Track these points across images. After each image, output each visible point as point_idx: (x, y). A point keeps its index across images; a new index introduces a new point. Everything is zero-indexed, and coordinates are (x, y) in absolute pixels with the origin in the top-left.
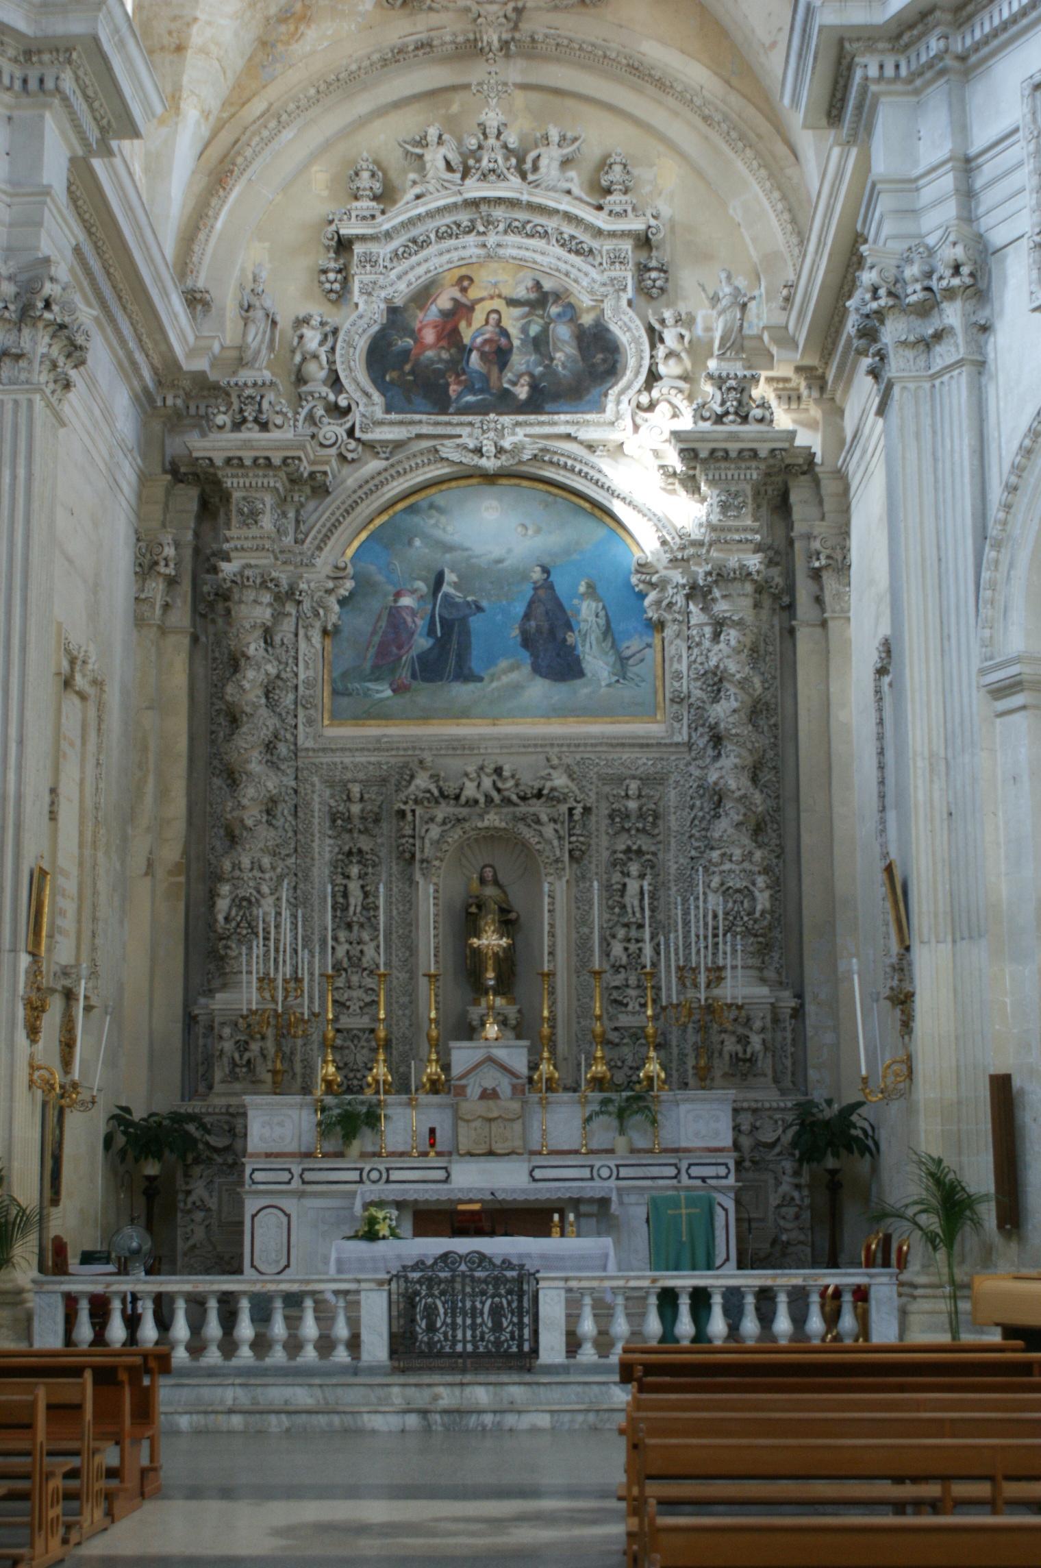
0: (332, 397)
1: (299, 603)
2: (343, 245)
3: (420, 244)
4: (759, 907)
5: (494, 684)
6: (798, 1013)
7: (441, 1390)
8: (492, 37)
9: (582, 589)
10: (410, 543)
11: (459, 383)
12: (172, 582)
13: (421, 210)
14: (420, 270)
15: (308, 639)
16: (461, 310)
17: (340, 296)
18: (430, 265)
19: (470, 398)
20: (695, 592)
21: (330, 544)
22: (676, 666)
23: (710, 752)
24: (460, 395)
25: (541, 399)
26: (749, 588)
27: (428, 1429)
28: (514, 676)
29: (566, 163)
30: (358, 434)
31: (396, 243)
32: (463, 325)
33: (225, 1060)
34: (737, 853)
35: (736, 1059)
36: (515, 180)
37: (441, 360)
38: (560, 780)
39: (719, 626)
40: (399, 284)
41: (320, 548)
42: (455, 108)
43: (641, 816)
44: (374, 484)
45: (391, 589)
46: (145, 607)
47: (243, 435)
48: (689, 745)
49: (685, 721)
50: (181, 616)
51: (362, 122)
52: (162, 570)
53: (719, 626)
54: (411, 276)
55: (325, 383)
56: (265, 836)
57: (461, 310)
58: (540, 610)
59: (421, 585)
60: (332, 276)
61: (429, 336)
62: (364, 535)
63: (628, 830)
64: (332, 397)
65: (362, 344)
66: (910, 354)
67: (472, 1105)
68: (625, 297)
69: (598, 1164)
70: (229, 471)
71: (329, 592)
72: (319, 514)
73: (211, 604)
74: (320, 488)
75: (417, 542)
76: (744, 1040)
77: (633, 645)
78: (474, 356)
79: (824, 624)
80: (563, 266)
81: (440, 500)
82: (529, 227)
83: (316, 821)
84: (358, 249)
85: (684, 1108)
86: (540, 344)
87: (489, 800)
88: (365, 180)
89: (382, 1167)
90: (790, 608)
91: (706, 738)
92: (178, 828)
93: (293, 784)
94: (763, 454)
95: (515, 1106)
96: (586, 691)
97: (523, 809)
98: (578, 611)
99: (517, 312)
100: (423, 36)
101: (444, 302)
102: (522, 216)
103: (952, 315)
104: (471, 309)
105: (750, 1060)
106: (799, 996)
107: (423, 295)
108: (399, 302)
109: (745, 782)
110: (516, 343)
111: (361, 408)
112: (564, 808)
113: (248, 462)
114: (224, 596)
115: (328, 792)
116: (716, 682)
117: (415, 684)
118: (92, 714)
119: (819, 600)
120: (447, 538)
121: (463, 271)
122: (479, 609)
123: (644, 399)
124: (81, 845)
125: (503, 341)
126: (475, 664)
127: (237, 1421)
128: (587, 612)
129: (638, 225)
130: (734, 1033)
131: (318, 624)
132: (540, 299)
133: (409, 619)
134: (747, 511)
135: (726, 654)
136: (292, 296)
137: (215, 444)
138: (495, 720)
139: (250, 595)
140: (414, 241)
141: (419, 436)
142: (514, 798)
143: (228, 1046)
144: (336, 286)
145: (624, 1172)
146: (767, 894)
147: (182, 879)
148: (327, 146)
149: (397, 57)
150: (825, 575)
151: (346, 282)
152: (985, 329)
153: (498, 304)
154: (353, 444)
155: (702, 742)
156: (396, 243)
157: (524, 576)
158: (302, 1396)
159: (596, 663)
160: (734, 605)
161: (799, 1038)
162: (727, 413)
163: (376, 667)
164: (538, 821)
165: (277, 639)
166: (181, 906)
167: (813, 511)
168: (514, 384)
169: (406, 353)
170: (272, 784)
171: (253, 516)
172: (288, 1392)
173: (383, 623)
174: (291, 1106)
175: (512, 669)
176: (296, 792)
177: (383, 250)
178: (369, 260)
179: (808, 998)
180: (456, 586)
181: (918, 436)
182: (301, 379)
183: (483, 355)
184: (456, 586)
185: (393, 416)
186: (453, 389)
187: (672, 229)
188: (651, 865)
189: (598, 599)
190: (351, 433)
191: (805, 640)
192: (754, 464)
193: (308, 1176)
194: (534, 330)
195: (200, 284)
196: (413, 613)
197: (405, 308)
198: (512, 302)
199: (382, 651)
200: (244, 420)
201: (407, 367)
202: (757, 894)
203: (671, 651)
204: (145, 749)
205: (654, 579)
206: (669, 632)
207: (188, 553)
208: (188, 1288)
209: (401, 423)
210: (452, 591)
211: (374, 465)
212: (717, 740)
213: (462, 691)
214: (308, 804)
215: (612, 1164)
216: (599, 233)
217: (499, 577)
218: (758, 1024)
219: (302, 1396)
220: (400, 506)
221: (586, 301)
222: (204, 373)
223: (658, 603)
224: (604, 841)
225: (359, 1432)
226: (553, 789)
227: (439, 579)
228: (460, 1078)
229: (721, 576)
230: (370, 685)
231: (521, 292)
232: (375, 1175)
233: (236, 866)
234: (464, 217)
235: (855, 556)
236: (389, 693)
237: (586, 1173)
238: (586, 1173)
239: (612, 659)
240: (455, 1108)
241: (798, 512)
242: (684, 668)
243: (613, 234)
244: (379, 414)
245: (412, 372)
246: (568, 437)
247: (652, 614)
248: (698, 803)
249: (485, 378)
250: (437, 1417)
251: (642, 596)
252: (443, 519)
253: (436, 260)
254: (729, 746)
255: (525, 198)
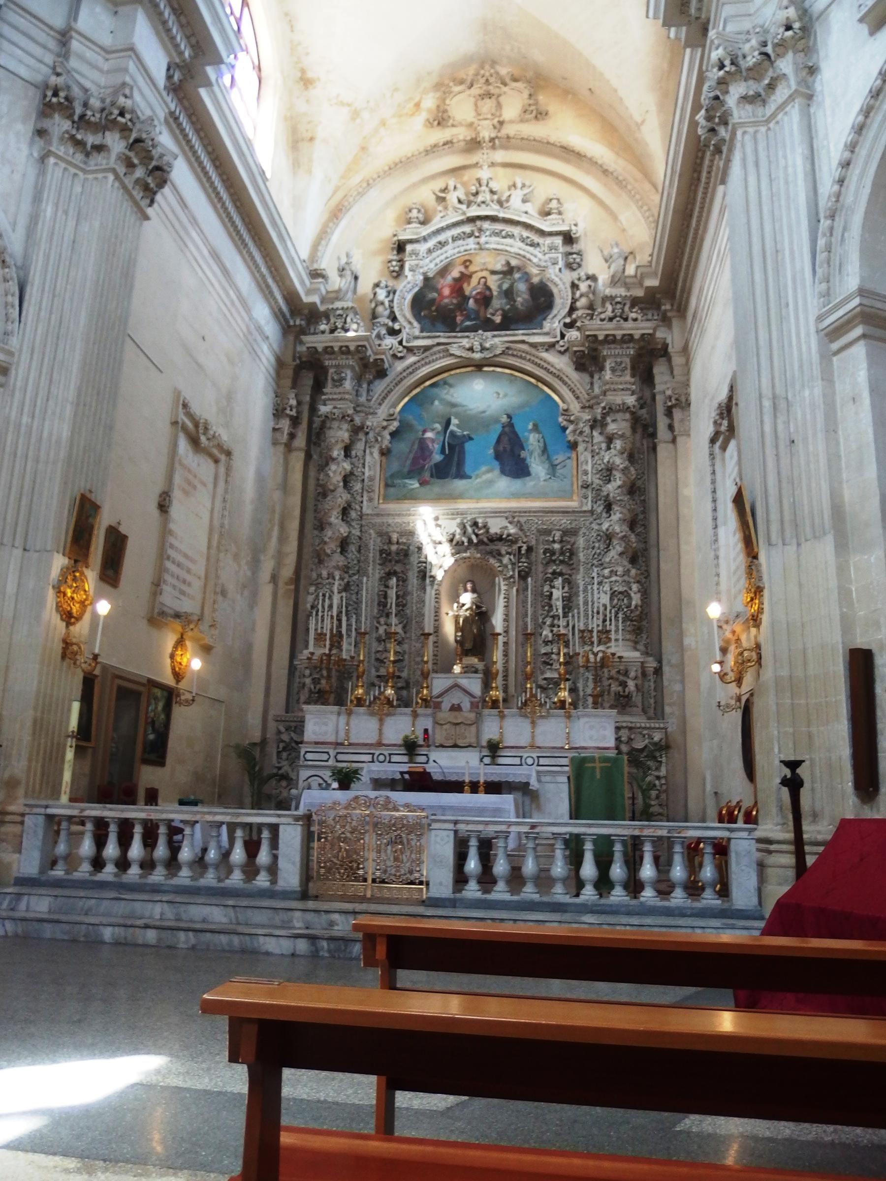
0: (390, 324)
1: (367, 433)
2: (400, 247)
3: (442, 244)
4: (634, 603)
5: (478, 480)
6: (658, 671)
7: (336, 917)
8: (486, 134)
9: (530, 427)
10: (432, 403)
11: (462, 315)
12: (295, 421)
13: (443, 224)
14: (443, 257)
15: (371, 454)
16: (465, 278)
17: (398, 274)
18: (448, 254)
19: (468, 323)
20: (595, 424)
21: (386, 401)
22: (584, 467)
23: (604, 515)
24: (462, 322)
25: (509, 322)
26: (628, 416)
27: (315, 955)
28: (489, 476)
29: (524, 201)
30: (404, 344)
31: (431, 244)
32: (465, 286)
33: (306, 690)
34: (620, 570)
35: (618, 695)
36: (497, 207)
37: (452, 304)
38: (512, 530)
39: (610, 440)
40: (431, 266)
41: (380, 404)
42: (466, 178)
43: (562, 553)
44: (412, 369)
45: (420, 428)
46: (278, 434)
47: (336, 334)
48: (592, 512)
49: (590, 499)
50: (301, 441)
51: (415, 186)
52: (288, 412)
53: (610, 440)
54: (438, 261)
55: (388, 318)
56: (338, 559)
57: (465, 278)
58: (505, 439)
59: (438, 427)
60: (394, 263)
61: (446, 292)
62: (406, 399)
63: (554, 561)
64: (390, 324)
65: (409, 297)
66: (749, 107)
67: (444, 714)
68: (557, 267)
69: (525, 755)
70: (327, 356)
71: (384, 428)
72: (380, 386)
73: (316, 436)
74: (382, 374)
75: (436, 403)
76: (624, 684)
77: (559, 458)
78: (471, 301)
79: (674, 441)
80: (522, 252)
81: (451, 381)
82: (504, 233)
83: (371, 555)
84: (409, 248)
85: (583, 720)
86: (509, 294)
87: (470, 541)
88: (415, 213)
89: (386, 753)
90: (654, 435)
91: (602, 508)
92: (291, 560)
93: (358, 534)
94: (637, 337)
95: (472, 716)
96: (532, 483)
97: (492, 547)
98: (527, 439)
99: (496, 277)
100: (449, 139)
101: (455, 273)
102: (498, 227)
103: (786, 65)
104: (470, 277)
105: (627, 696)
106: (660, 661)
107: (443, 271)
108: (431, 275)
109: (625, 528)
110: (495, 293)
111: (407, 330)
112: (515, 547)
113: (336, 349)
114: (323, 426)
115: (379, 539)
116: (607, 473)
117: (433, 480)
118: (222, 470)
119: (671, 427)
120: (453, 400)
121: (467, 258)
122: (471, 439)
123: (568, 320)
124: (209, 547)
125: (488, 293)
126: (468, 469)
127: (151, 936)
128: (533, 440)
129: (564, 228)
130: (617, 679)
131: (377, 446)
132: (509, 270)
133: (430, 445)
134: (628, 372)
135: (615, 457)
136: (371, 271)
137: (317, 341)
138: (478, 500)
139: (335, 424)
140: (440, 243)
141: (439, 344)
142: (485, 540)
143: (308, 681)
144: (397, 269)
145: (542, 761)
146: (639, 595)
147: (292, 587)
148: (395, 198)
149: (432, 150)
150: (674, 410)
151: (402, 267)
152: (813, 70)
153: (485, 274)
154: (401, 348)
155: (599, 510)
156: (431, 244)
157: (496, 420)
158: (217, 915)
159: (538, 468)
160: (618, 425)
161: (659, 687)
162: (615, 317)
163: (410, 472)
164: (500, 554)
165: (353, 453)
166: (291, 602)
167: (667, 378)
168: (493, 315)
169: (433, 301)
170: (344, 530)
171: (339, 382)
172: (206, 911)
173: (416, 447)
174: (332, 713)
175: (488, 471)
176: (360, 538)
177: (422, 248)
178: (415, 253)
179: (664, 663)
180: (458, 426)
181: (757, 164)
182: (374, 316)
183: (476, 301)
184: (458, 426)
185: (425, 334)
186: (459, 319)
187: (585, 235)
188: (569, 582)
189: (539, 433)
190: (400, 343)
191: (663, 451)
192: (631, 345)
193: (340, 757)
194: (505, 286)
195: (322, 267)
196: (433, 441)
197: (434, 278)
198: (493, 273)
199: (415, 461)
200: (336, 328)
201: (434, 308)
202: (632, 595)
203: (581, 458)
204: (274, 511)
205: (572, 418)
206: (581, 448)
207: (306, 409)
208: (143, 815)
209: (429, 337)
210: (455, 429)
211: (412, 359)
212: (608, 507)
213: (460, 484)
214: (366, 545)
215: (535, 755)
216: (542, 233)
217: (481, 422)
218: (632, 674)
219: (217, 915)
220: (428, 383)
221: (534, 271)
222: (314, 304)
223: (574, 431)
224: (540, 568)
225: (255, 952)
226: (509, 535)
227: (448, 423)
228: (438, 697)
229: (610, 410)
230: (407, 481)
231: (499, 267)
232: (381, 758)
233: (320, 576)
234: (467, 229)
235: (693, 398)
236: (417, 485)
237: (517, 761)
238: (517, 761)
239: (547, 465)
240: (434, 716)
241: (658, 379)
242: (589, 468)
243: (551, 234)
244: (417, 332)
245: (436, 310)
246: (523, 342)
247: (571, 438)
248: (597, 545)
249: (477, 313)
250: (325, 944)
251: (564, 429)
252: (452, 390)
253: (451, 251)
254: (616, 508)
255: (501, 215)
